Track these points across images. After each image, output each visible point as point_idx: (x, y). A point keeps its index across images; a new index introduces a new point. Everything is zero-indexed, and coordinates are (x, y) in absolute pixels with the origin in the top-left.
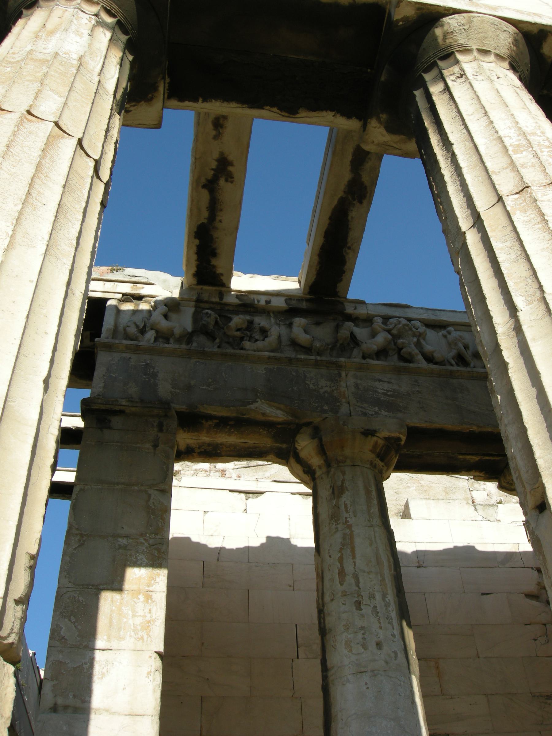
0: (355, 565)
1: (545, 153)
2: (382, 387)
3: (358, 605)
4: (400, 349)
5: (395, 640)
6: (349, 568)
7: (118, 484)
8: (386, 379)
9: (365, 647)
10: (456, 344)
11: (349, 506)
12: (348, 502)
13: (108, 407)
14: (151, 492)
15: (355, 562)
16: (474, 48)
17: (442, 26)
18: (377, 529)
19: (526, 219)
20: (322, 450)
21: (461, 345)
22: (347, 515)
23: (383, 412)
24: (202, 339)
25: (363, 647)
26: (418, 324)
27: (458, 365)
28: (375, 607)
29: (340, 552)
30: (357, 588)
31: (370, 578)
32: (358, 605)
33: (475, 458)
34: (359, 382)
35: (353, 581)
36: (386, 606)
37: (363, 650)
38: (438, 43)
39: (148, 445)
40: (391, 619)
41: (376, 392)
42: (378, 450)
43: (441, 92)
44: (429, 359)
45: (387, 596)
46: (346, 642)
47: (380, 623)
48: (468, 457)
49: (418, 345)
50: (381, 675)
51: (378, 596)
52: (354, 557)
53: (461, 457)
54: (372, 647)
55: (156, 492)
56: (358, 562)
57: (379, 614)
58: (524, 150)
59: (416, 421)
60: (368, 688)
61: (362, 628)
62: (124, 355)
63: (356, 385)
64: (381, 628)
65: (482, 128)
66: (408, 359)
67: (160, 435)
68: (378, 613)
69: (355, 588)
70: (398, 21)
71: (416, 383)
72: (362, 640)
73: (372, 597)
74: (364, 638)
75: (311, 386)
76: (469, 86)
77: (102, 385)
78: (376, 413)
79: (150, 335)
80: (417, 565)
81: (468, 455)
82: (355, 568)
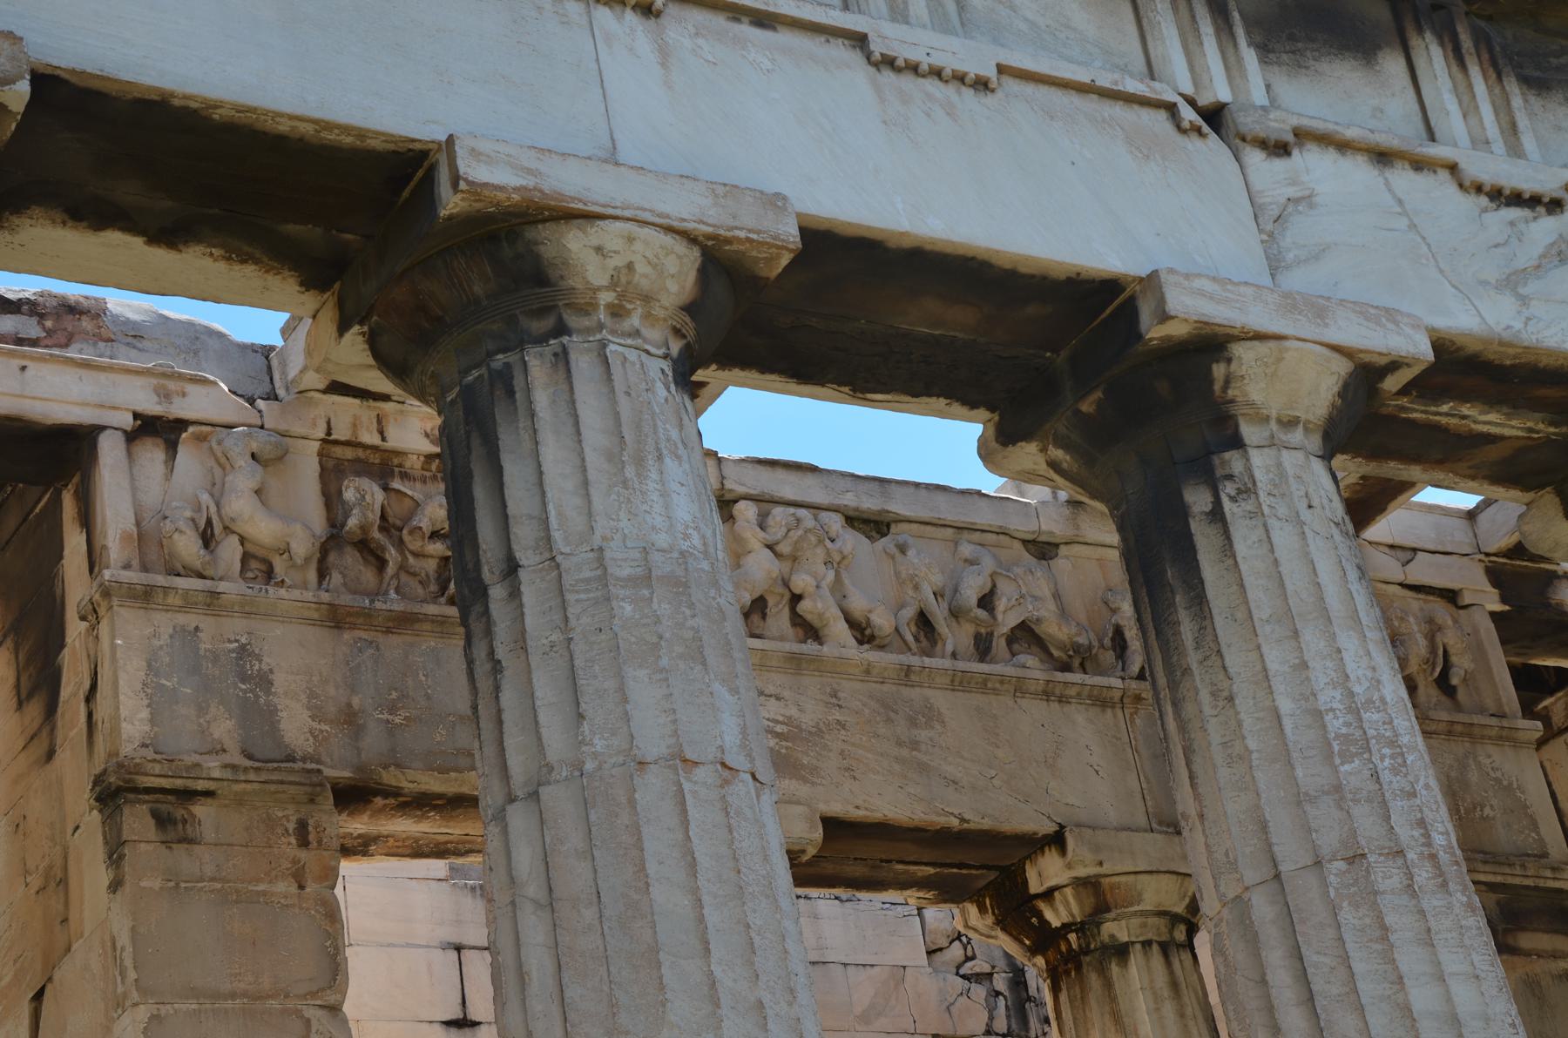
1: (1387, 762)
4: (796, 598)
7: (233, 995)
13: (179, 783)
14: (310, 1013)
16: (1274, 414)
17: (1229, 361)
19: (1356, 922)
24: (349, 561)
38: (1212, 391)
39: (285, 887)
43: (1207, 514)
44: (862, 632)
49: (838, 589)
55: (320, 1013)
58: (1356, 754)
59: (837, 809)
62: (190, 620)
65: (1286, 668)
66: (810, 631)
67: (303, 855)
70: (1151, 339)
71: (834, 700)
76: (1261, 530)
77: (145, 714)
79: (230, 551)
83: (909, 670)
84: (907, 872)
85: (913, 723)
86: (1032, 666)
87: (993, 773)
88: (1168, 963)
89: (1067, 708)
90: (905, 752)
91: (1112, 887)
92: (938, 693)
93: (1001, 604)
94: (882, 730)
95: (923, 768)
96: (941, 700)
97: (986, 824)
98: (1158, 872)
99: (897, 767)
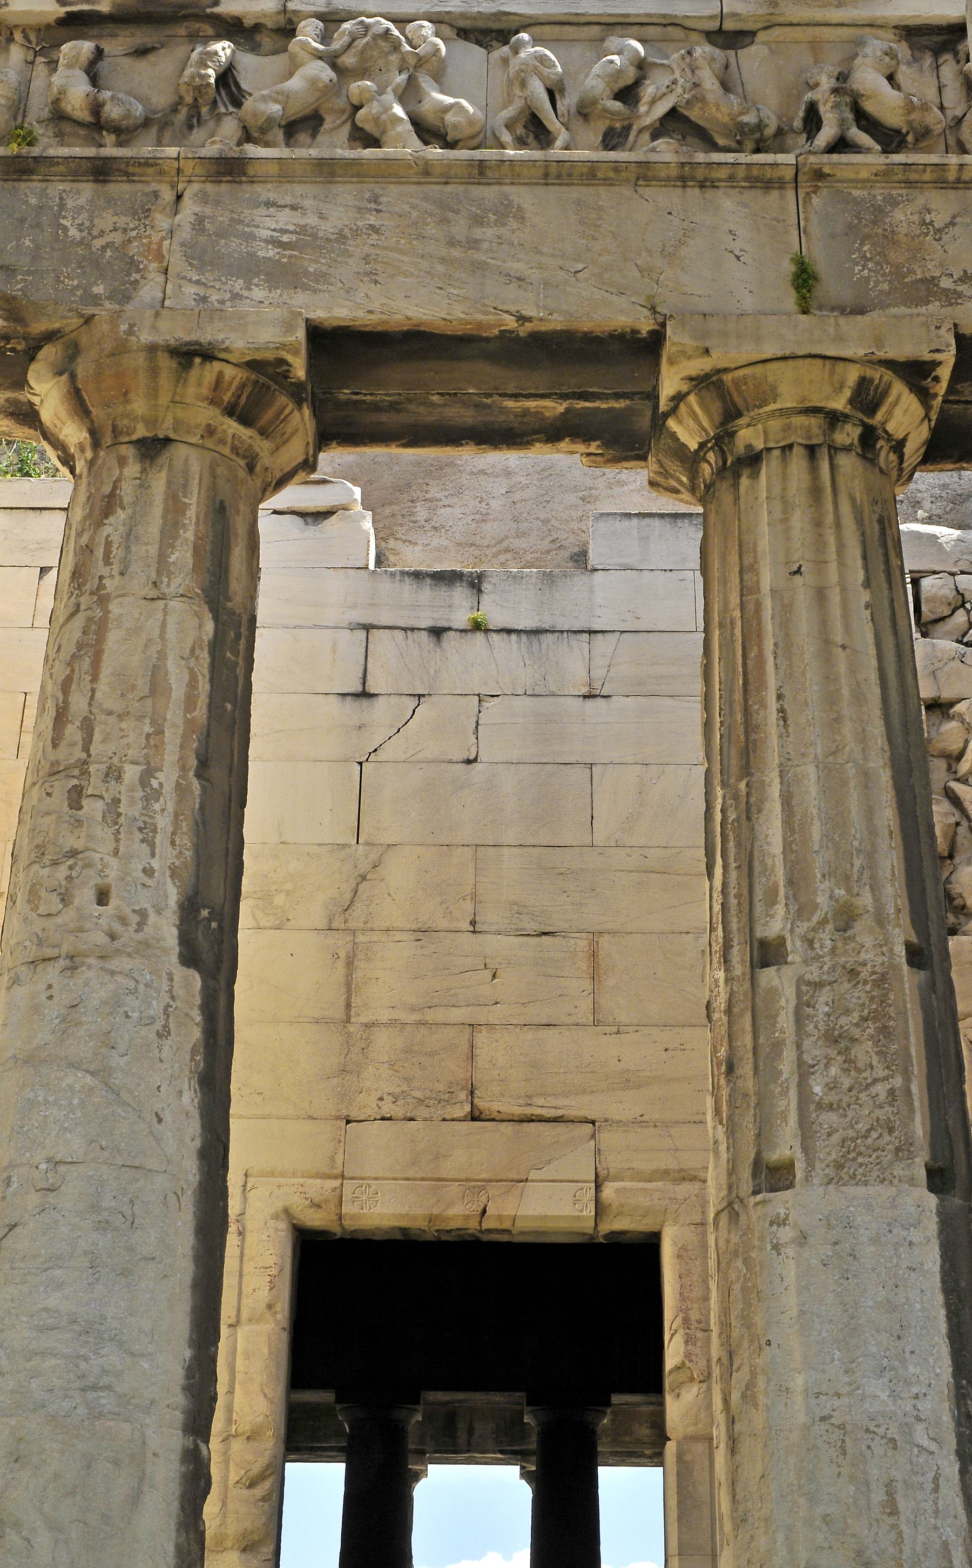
0: (92, 697)
2: (269, 223)
3: (76, 797)
5: (149, 882)
6: (79, 703)
8: (288, 200)
9: (65, 899)
10: (523, 85)
11: (115, 546)
12: (116, 539)
15: (93, 691)
18: (175, 604)
20: (78, 403)
21: (538, 89)
22: (105, 571)
23: (258, 293)
25: (63, 900)
26: (428, 28)
27: (521, 143)
28: (116, 801)
29: (69, 664)
30: (84, 755)
31: (122, 730)
32: (76, 797)
33: (554, 408)
34: (208, 211)
35: (79, 737)
36: (147, 799)
37: (61, 906)
40: (155, 831)
41: (252, 237)
42: (227, 397)
44: (426, 131)
45: (158, 774)
46: (33, 885)
47: (117, 840)
48: (532, 404)
50: (90, 967)
51: (131, 773)
52: (95, 678)
53: (510, 403)
54: (85, 896)
56: (103, 687)
57: (122, 820)
59: (337, 310)
60: (50, 998)
61: (73, 853)
63: (199, 221)
64: (116, 853)
68: (119, 815)
69: (79, 754)
71: (373, 206)
72: (64, 883)
73: (113, 774)
74: (69, 878)
75: (73, 232)
78: (235, 296)
80: (584, 690)
81: (528, 396)
82: (90, 705)
83: (482, 165)
84: (526, 412)
85: (478, 221)
86: (666, 151)
87: (580, 266)
88: (814, 470)
89: (710, 193)
90: (456, 253)
91: (736, 383)
92: (522, 189)
93: (649, 90)
94: (431, 231)
95: (479, 267)
96: (522, 196)
97: (556, 323)
98: (794, 357)
99: (440, 268)
